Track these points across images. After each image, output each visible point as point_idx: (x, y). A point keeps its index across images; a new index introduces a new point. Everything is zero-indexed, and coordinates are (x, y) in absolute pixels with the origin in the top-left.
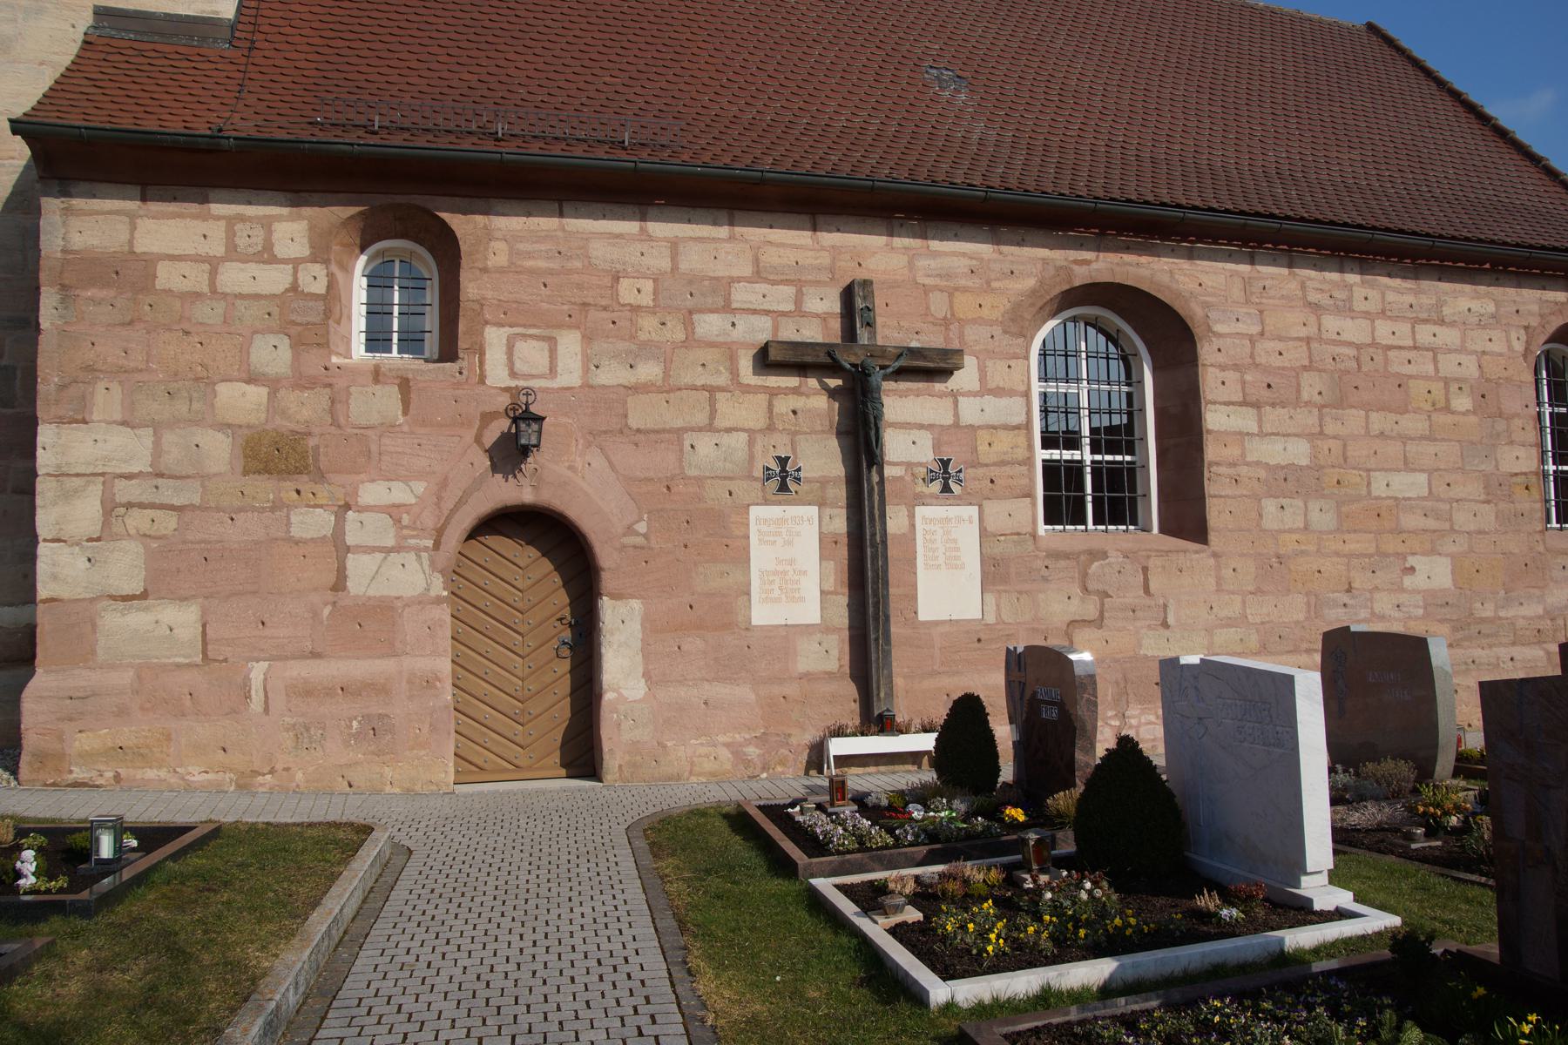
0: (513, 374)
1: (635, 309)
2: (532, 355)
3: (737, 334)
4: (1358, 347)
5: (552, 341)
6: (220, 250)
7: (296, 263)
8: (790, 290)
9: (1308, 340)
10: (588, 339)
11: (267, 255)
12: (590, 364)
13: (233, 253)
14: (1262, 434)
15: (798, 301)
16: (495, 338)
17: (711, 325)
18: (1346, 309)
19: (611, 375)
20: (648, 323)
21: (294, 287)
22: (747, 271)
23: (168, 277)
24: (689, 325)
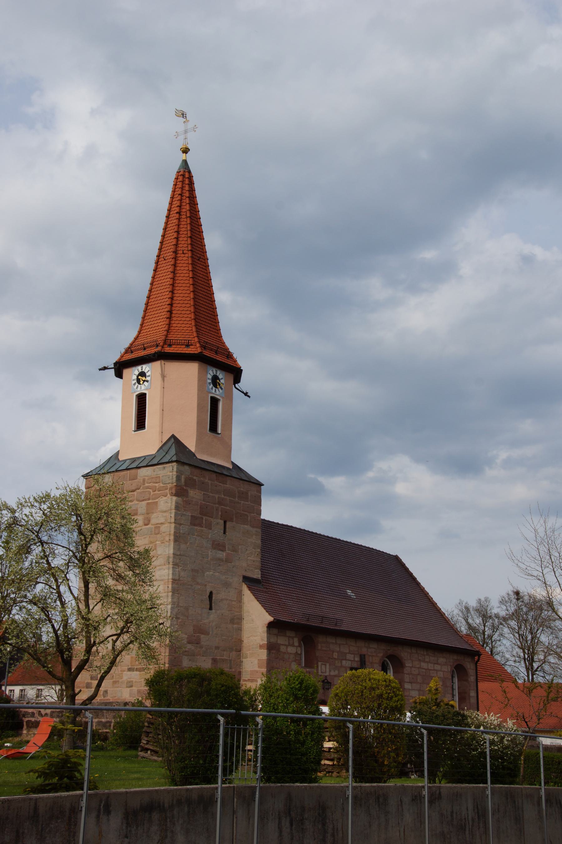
0: (322, 672)
1: (335, 659)
2: (323, 667)
3: (347, 665)
4: (426, 669)
5: (325, 665)
6: (287, 643)
7: (297, 647)
8: (353, 655)
9: (418, 668)
10: (330, 665)
11: (293, 645)
12: (330, 671)
13: (289, 645)
14: (412, 690)
15: (354, 658)
16: (320, 664)
17: (344, 662)
18: (424, 661)
19: (333, 673)
20: (337, 662)
21: (296, 652)
22: (348, 651)
23: (283, 649)
24: (341, 662)
